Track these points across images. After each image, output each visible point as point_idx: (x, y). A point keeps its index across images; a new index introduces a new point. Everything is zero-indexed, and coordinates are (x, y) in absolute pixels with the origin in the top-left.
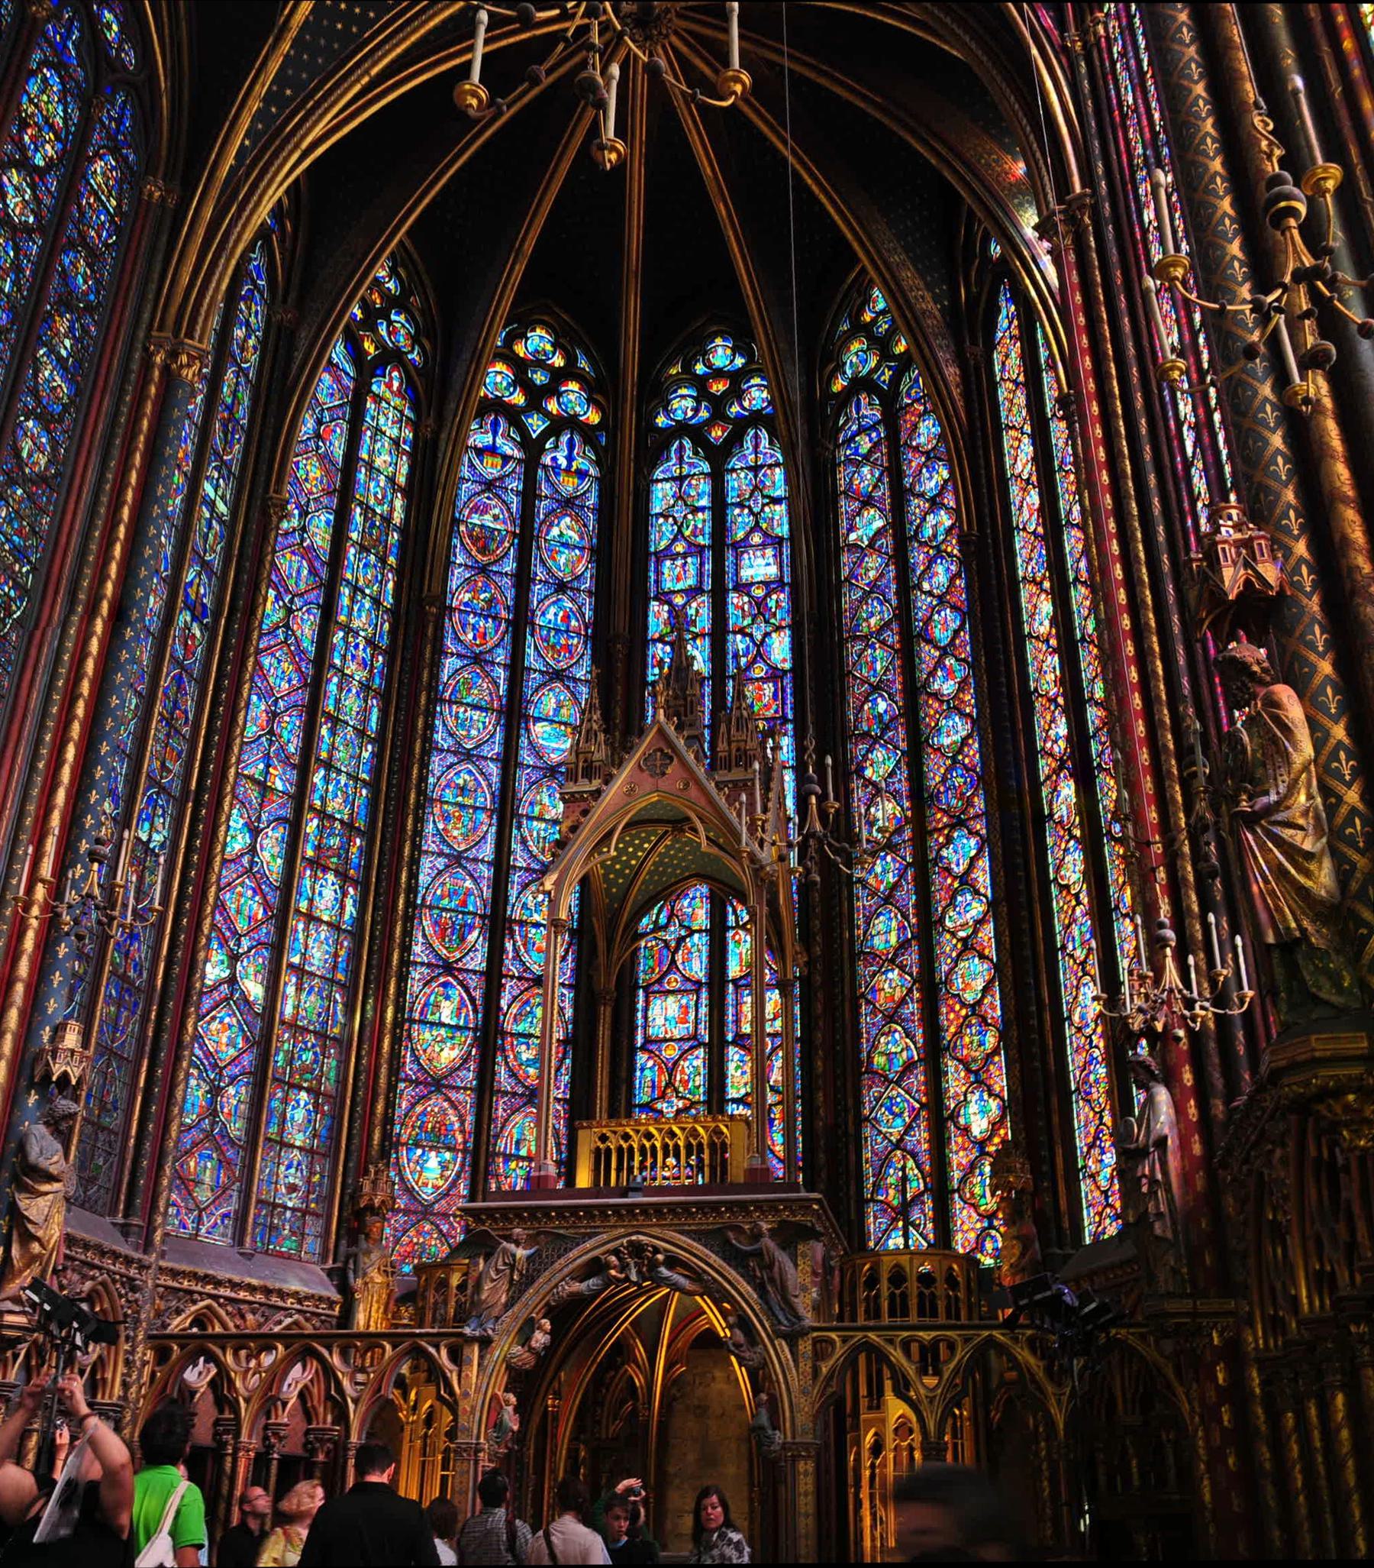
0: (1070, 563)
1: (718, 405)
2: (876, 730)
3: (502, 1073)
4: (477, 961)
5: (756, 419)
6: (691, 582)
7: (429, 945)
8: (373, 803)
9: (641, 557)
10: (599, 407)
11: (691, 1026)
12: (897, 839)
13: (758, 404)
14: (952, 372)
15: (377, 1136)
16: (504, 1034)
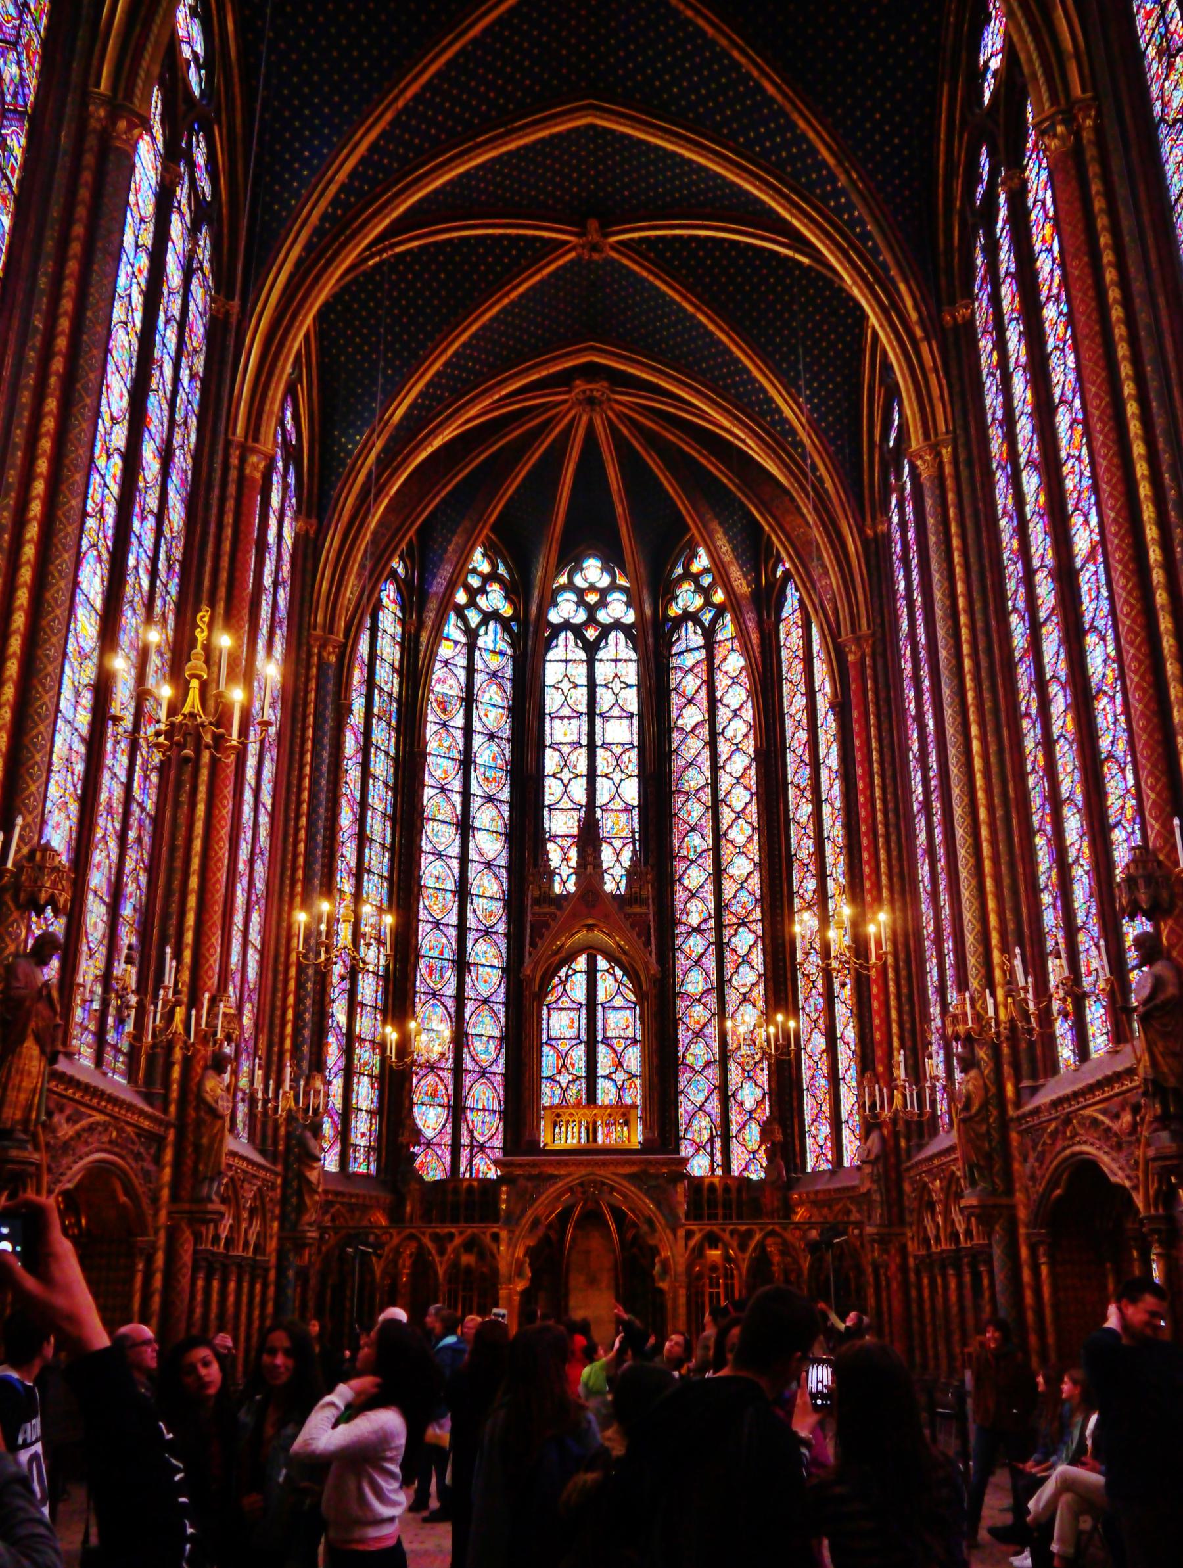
0: (824, 787)
1: (591, 610)
2: (692, 856)
3: (467, 1058)
4: (451, 990)
5: (617, 625)
6: (575, 739)
7: (423, 981)
8: (390, 891)
9: (541, 715)
10: (512, 602)
11: (575, 1031)
12: (703, 926)
13: (617, 614)
14: (755, 637)
15: (407, 1103)
16: (467, 1034)
